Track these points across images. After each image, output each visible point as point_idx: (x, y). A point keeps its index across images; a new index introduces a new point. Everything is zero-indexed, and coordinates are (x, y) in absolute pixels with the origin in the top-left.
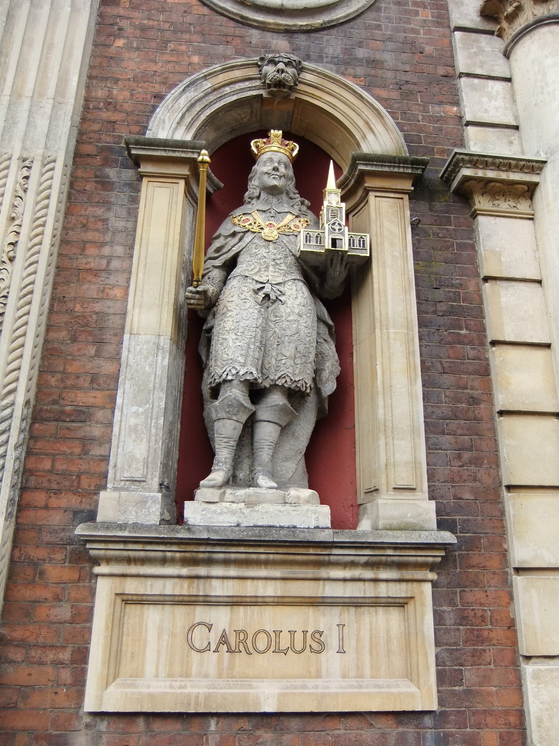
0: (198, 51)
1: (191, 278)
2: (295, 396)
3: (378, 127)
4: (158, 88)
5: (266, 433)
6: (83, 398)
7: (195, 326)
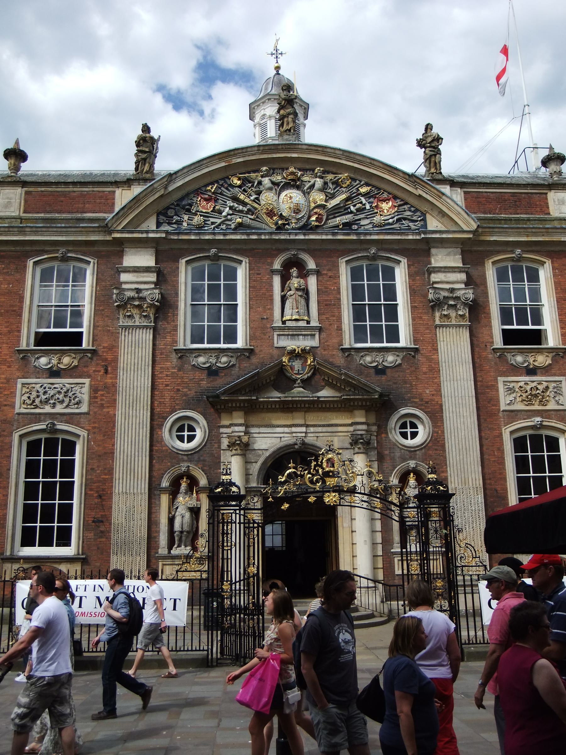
0: (169, 462)
1: (170, 512)
2: (188, 532)
3: (203, 479)
4: (163, 472)
5: (184, 538)
6: (155, 535)
7: (171, 521)
